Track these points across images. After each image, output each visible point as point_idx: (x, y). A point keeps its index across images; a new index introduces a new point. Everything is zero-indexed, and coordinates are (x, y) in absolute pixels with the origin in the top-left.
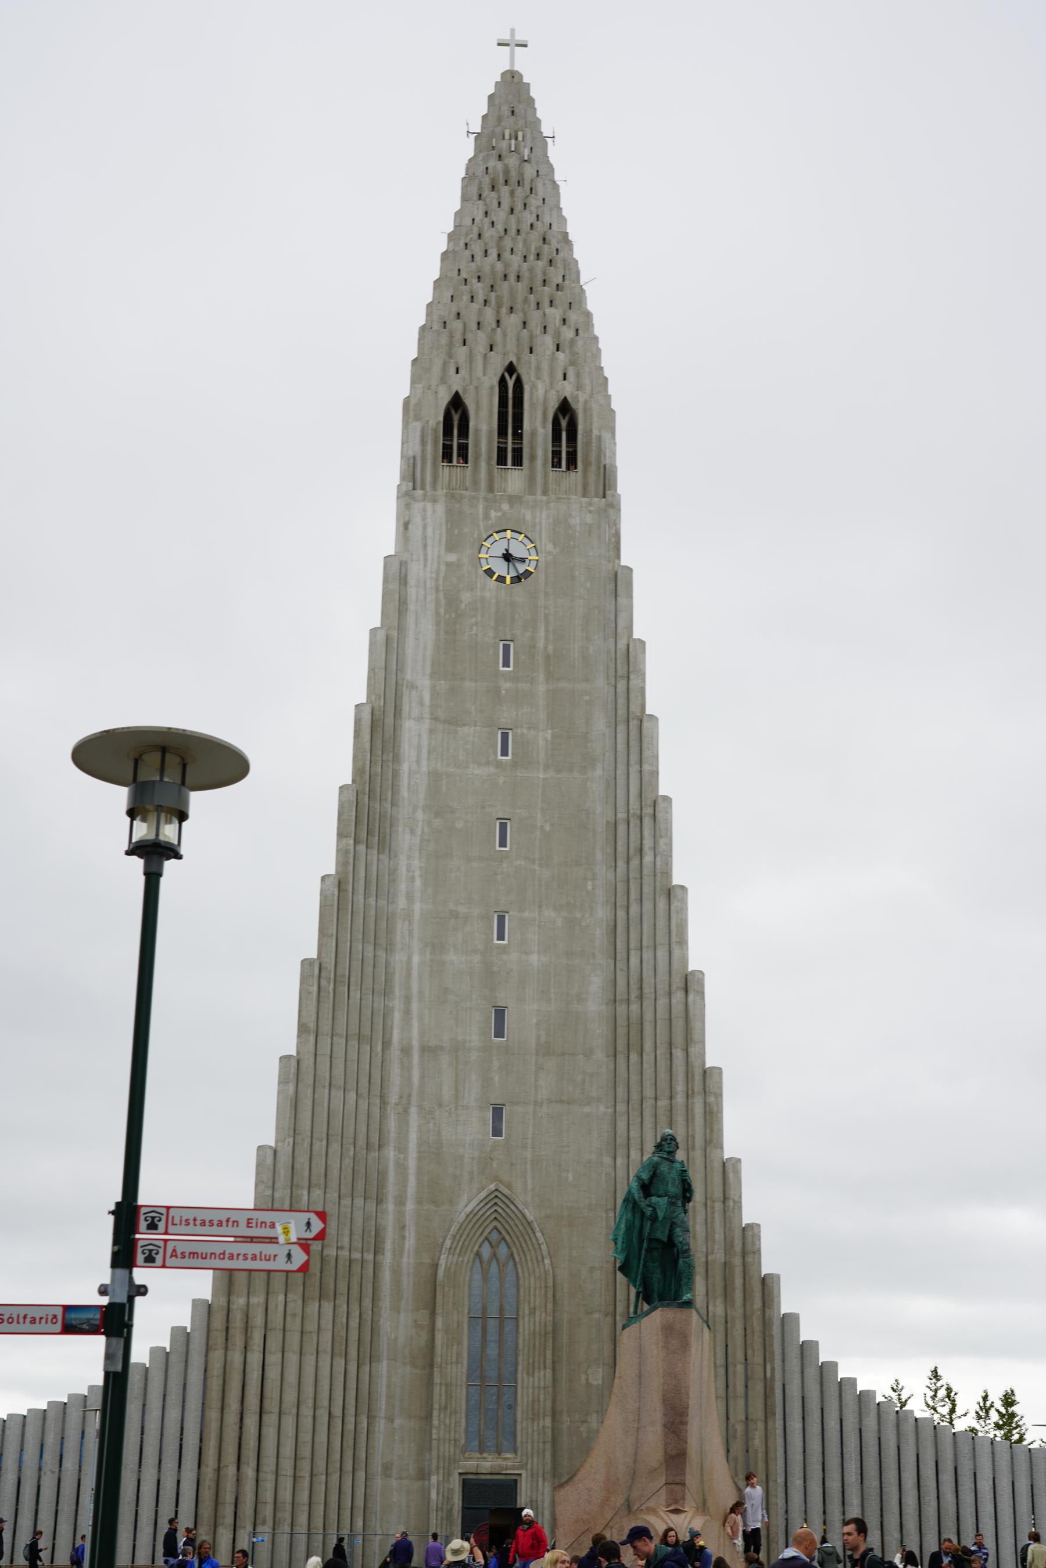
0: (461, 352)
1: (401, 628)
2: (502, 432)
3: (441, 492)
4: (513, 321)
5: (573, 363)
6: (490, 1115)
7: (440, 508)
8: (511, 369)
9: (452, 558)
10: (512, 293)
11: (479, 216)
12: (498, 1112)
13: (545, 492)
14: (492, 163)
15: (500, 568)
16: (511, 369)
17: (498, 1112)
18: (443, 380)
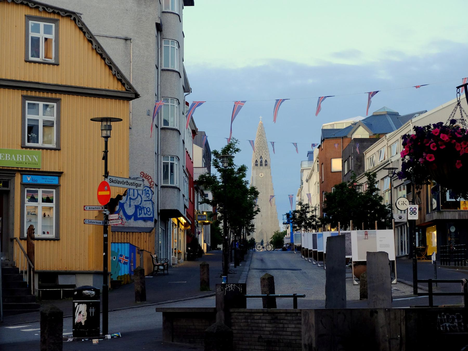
0: (257, 155)
1: (253, 183)
2: (261, 163)
3: (255, 169)
4: (261, 152)
5: (266, 156)
6: (261, 223)
7: (255, 171)
8: (261, 156)
9: (257, 176)
10: (261, 148)
11: (258, 139)
12: (262, 223)
13: (264, 169)
14: (259, 133)
15: (261, 176)
16: (261, 156)
17: (262, 223)
18: (255, 158)
